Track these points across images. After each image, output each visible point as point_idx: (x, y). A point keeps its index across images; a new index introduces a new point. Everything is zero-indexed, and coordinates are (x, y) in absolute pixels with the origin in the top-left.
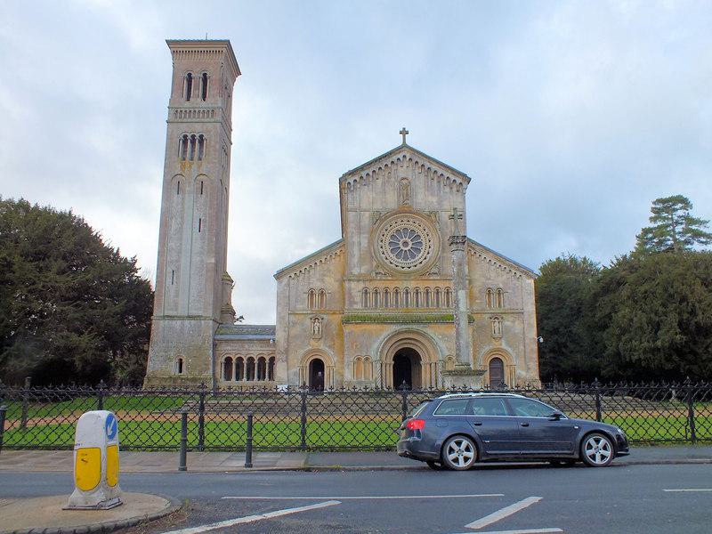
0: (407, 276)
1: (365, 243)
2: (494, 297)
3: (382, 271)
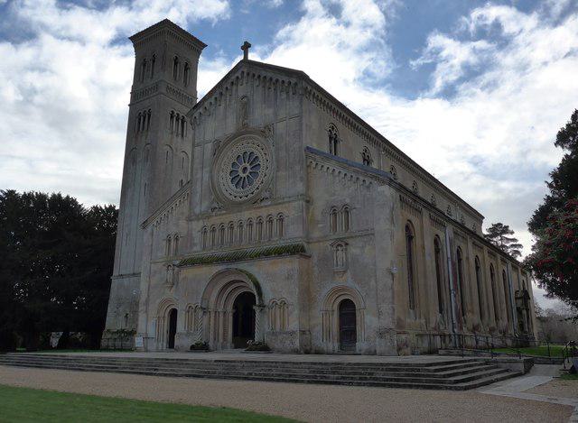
0: (238, 206)
1: (206, 176)
2: (341, 218)
3: (221, 204)
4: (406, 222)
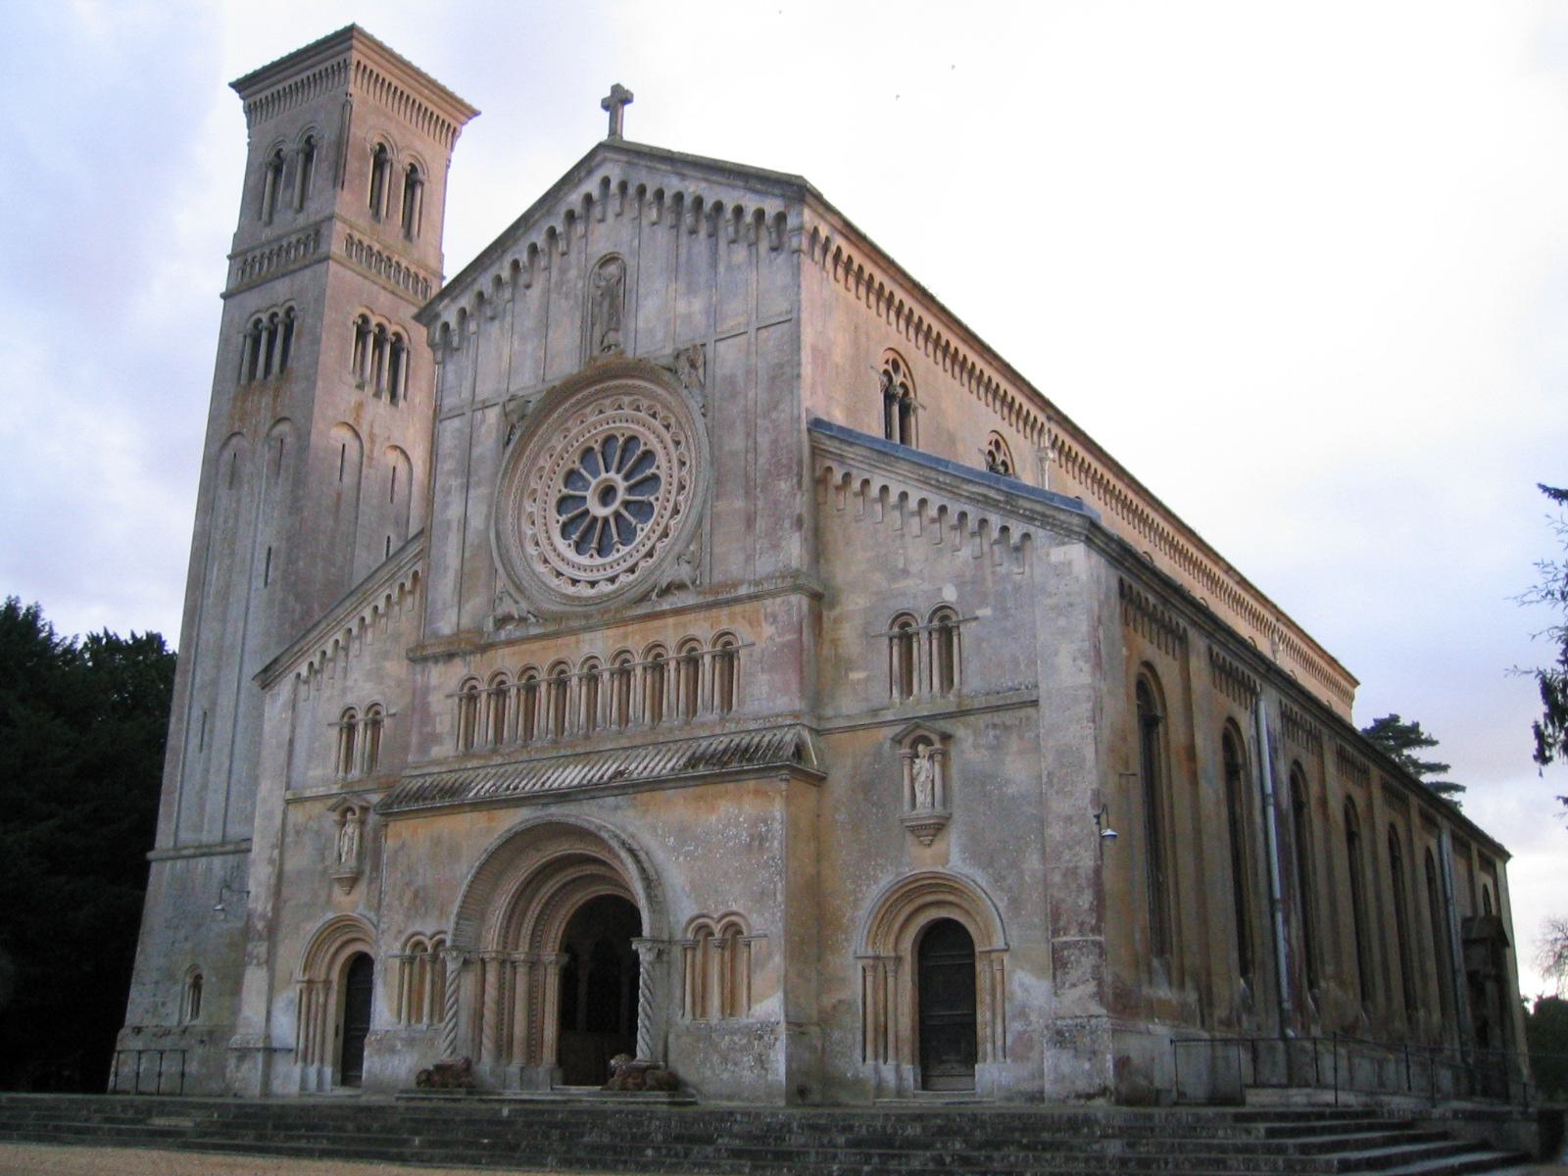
1: (477, 522)
2: (925, 650)
4: (1135, 668)
